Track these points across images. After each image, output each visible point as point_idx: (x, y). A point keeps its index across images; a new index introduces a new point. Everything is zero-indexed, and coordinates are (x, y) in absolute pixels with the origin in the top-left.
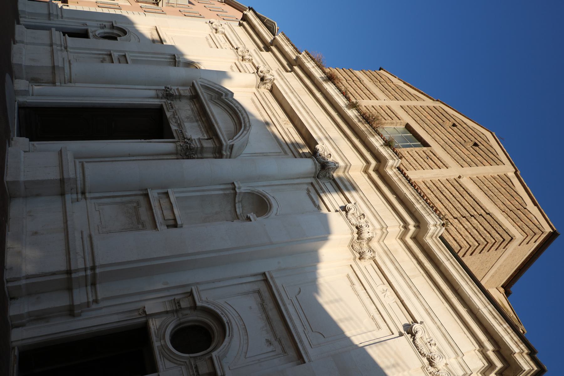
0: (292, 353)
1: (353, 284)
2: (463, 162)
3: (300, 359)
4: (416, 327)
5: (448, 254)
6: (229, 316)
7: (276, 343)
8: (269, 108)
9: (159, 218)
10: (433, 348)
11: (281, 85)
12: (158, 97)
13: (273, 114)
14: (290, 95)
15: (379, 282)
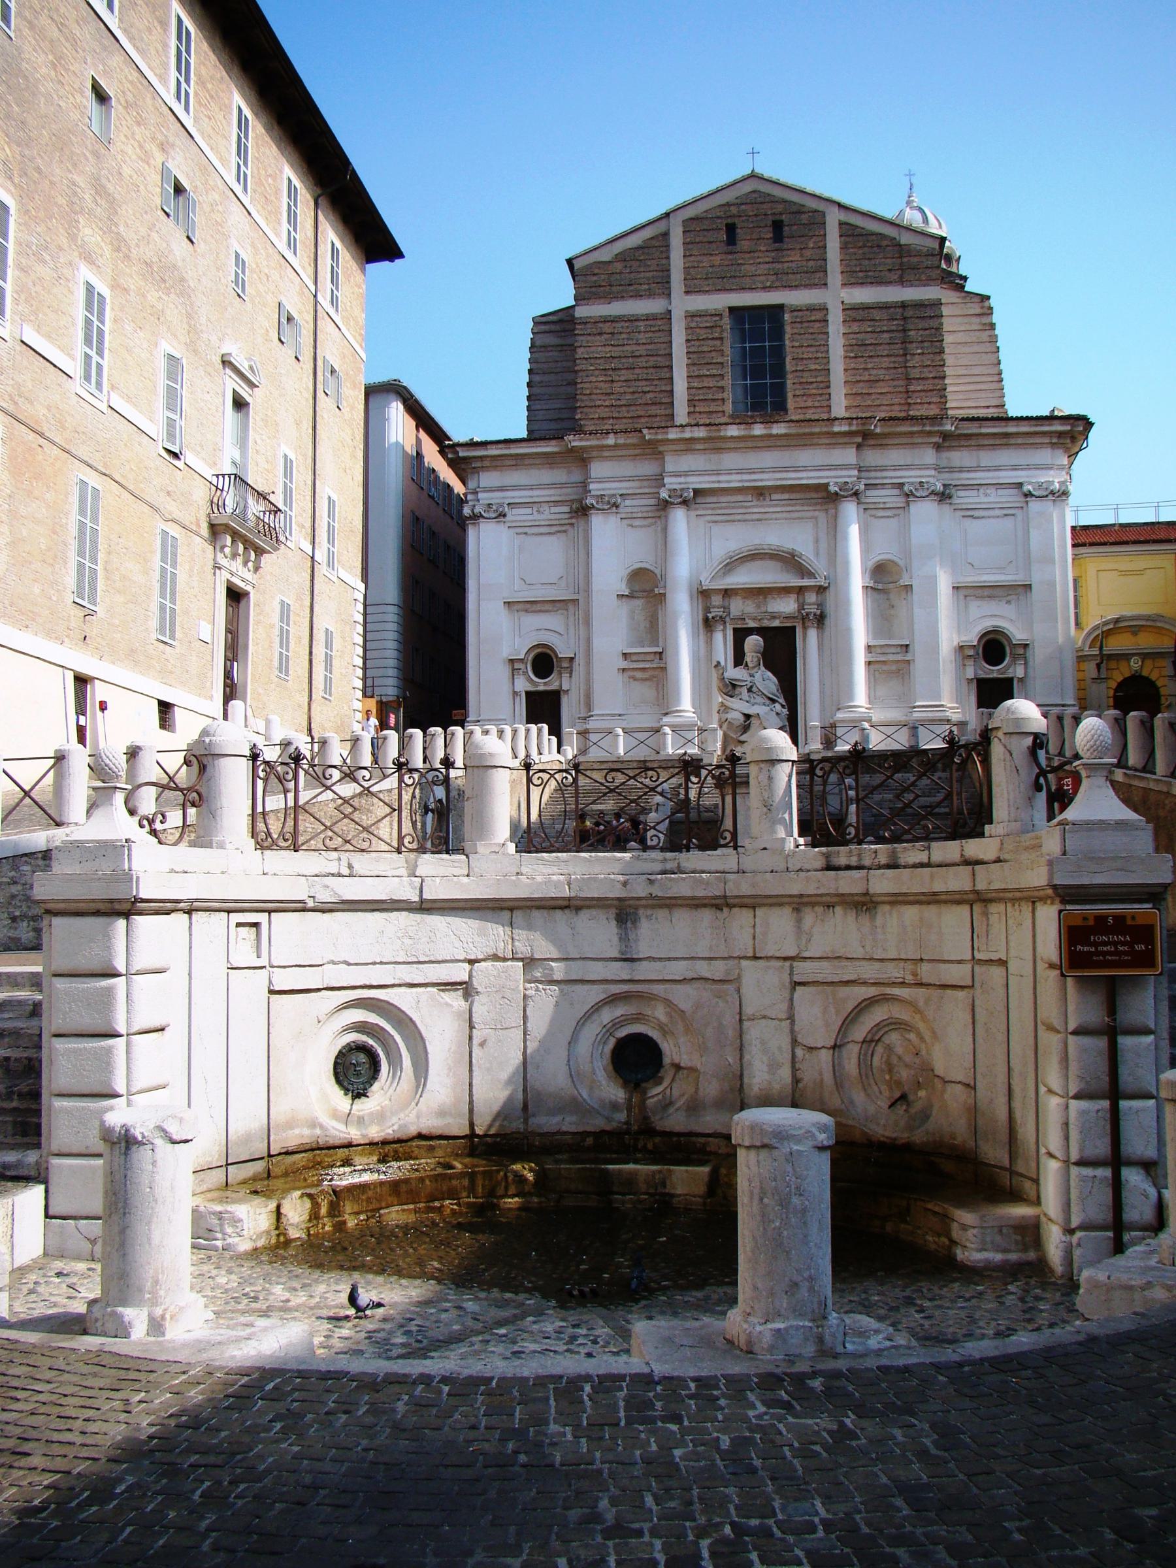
0: (1020, 590)
1: (972, 516)
2: (816, 276)
3: (1028, 587)
4: (1028, 488)
5: (976, 424)
6: (989, 624)
7: (1009, 598)
8: (733, 508)
9: (899, 657)
10: (1044, 486)
11: (700, 483)
12: (724, 630)
13: (746, 507)
14: (722, 478)
15: (974, 493)
